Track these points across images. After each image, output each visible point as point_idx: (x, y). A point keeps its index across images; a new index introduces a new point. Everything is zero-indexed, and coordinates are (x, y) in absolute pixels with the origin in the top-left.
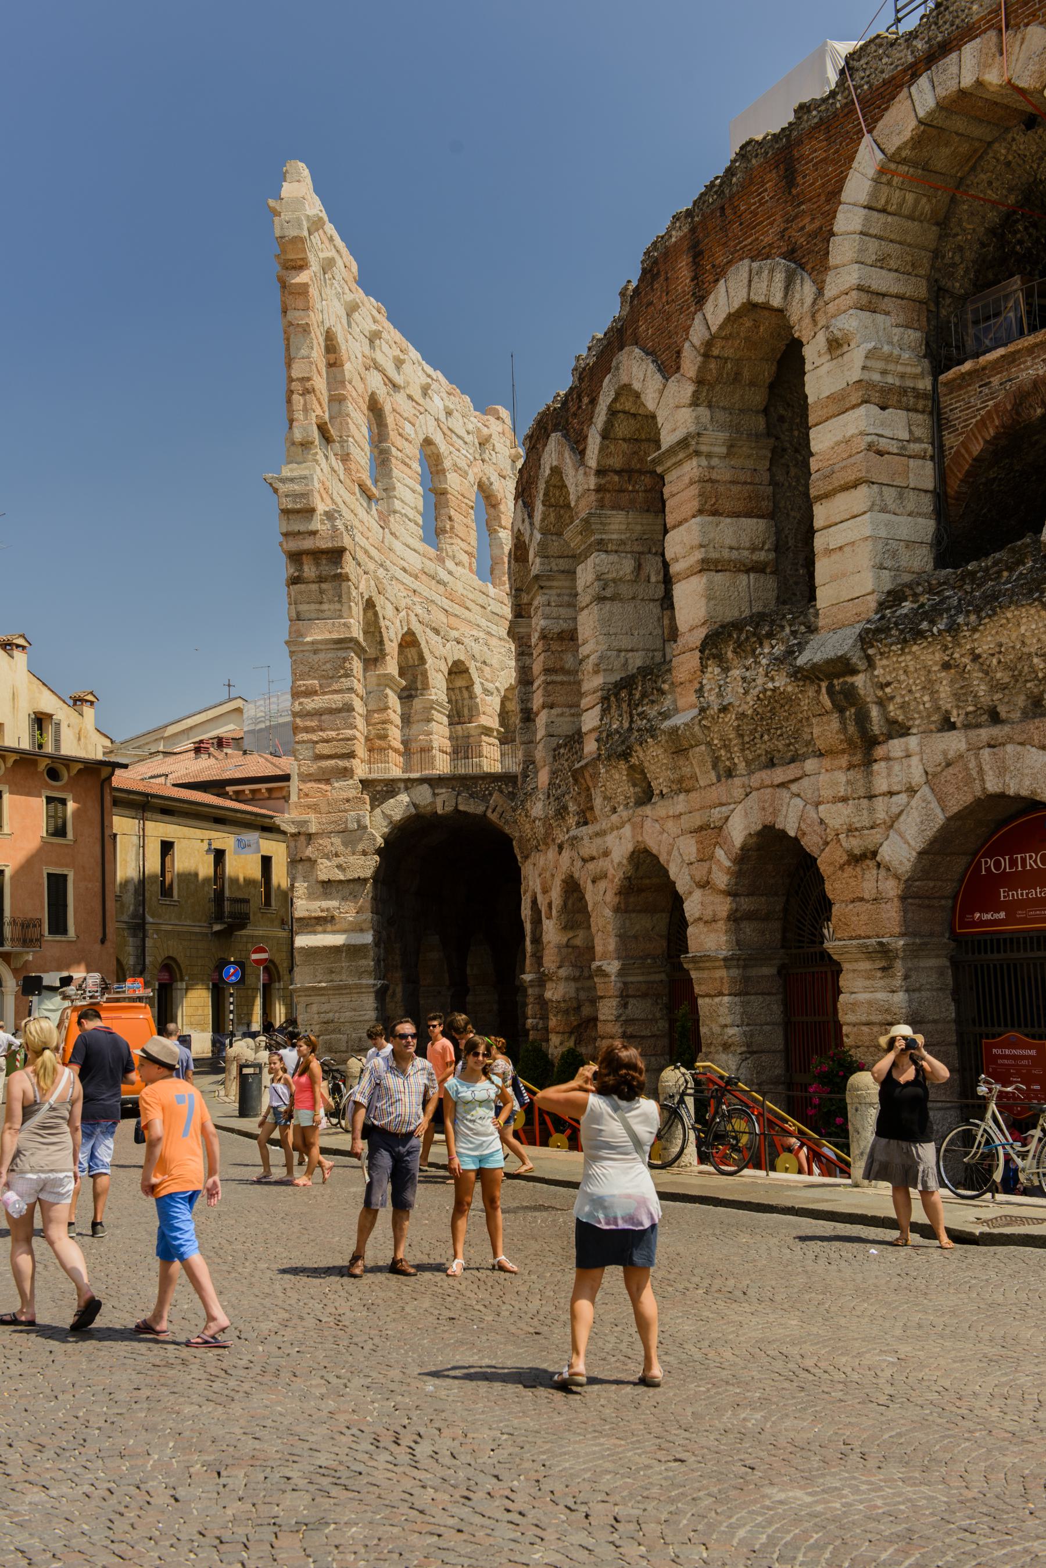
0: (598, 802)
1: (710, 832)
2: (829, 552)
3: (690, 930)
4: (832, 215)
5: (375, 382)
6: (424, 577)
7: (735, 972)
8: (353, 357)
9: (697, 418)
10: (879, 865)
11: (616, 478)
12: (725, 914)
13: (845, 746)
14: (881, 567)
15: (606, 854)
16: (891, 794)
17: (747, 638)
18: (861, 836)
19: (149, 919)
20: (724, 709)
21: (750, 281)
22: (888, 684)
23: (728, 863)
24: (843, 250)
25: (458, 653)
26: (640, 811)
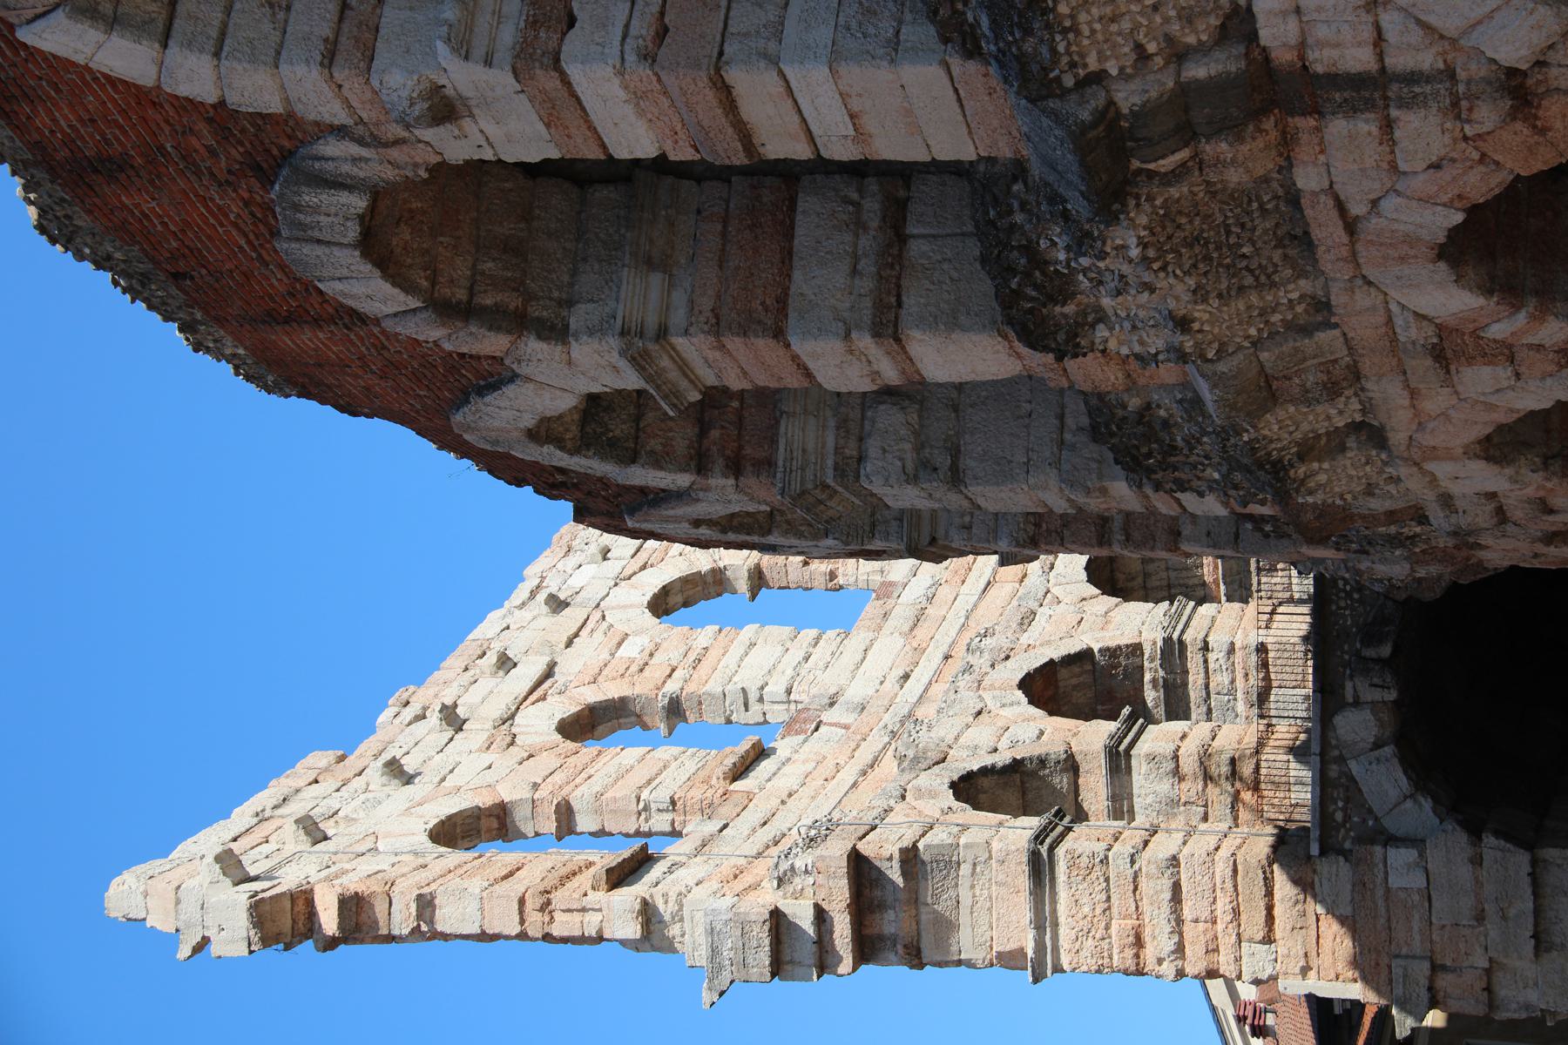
0: (1377, 505)
1: (1448, 349)
2: (860, 135)
4: (189, 105)
5: (539, 722)
6: (922, 633)
8: (490, 776)
9: (591, 332)
11: (715, 434)
13: (1269, 124)
14: (895, 43)
15: (1492, 496)
16: (1379, 39)
17: (1036, 287)
20: (1183, 324)
21: (319, 241)
22: (1139, 48)
23: (1521, 318)
24: (255, 90)
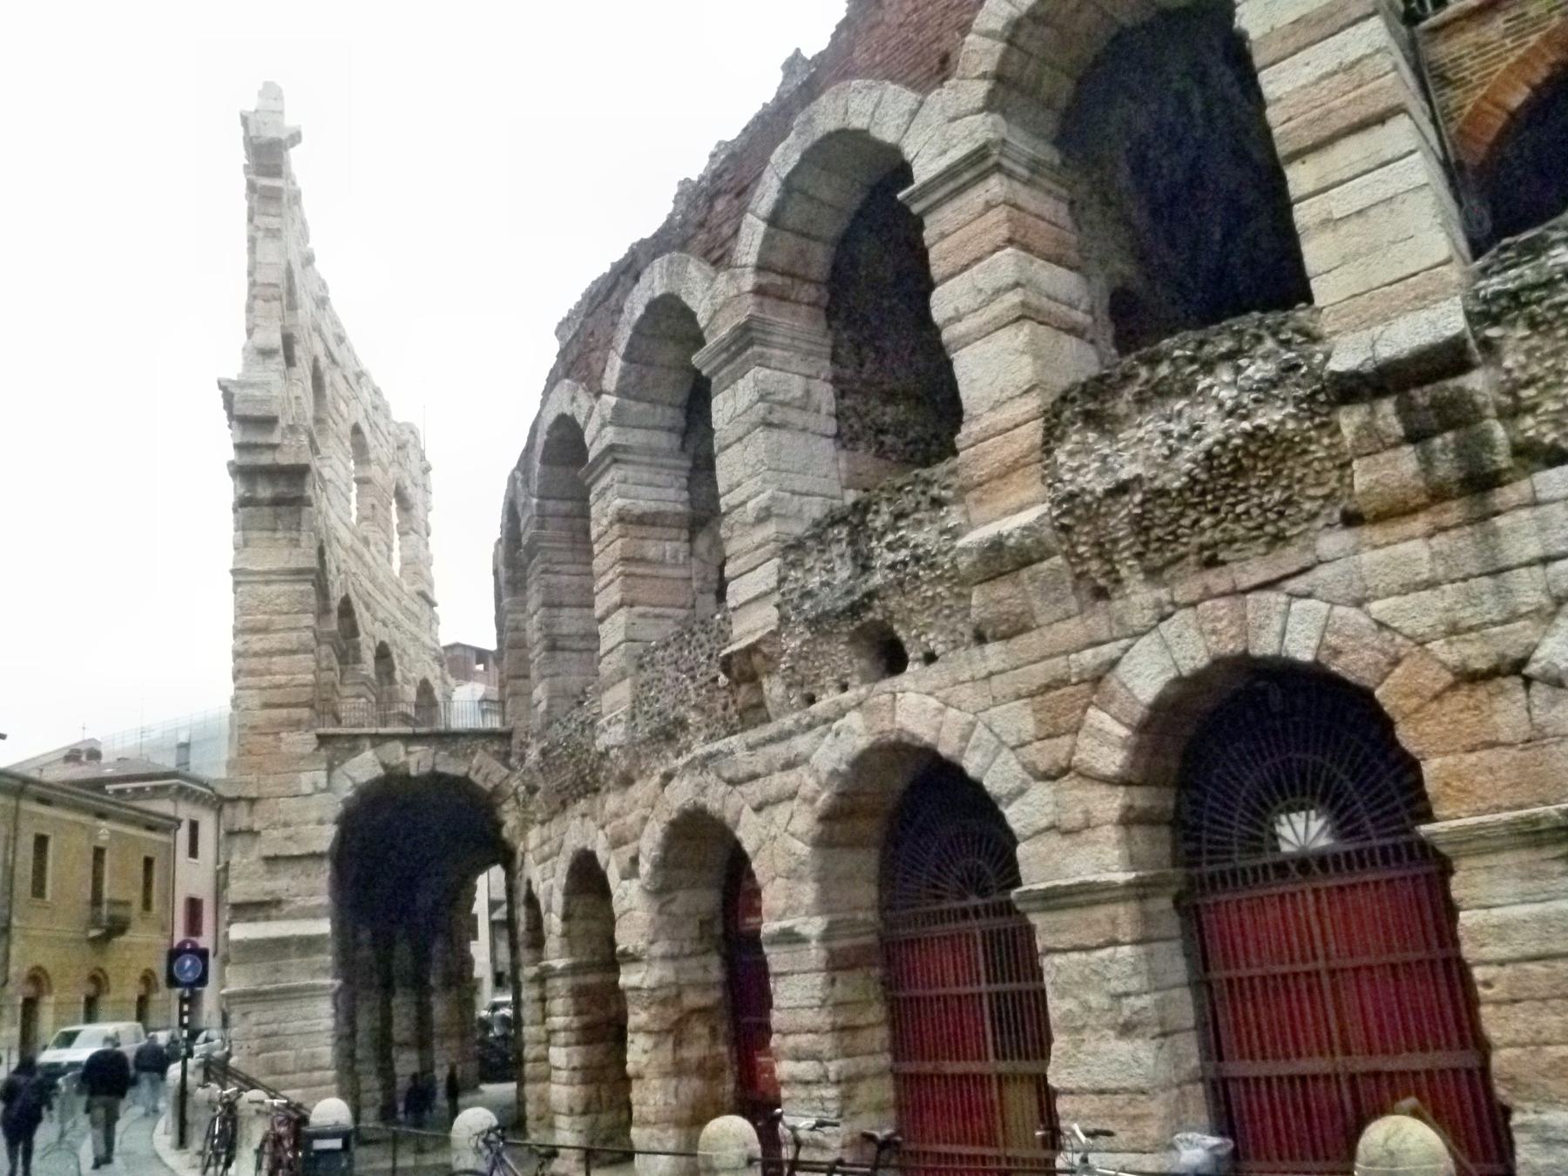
2: (1329, 223)
3: (1022, 851)
7: (1133, 906)
10: (1528, 681)
12: (1115, 815)
18: (1486, 640)
19: (15, 921)
22: (1529, 383)
23: (1124, 732)
25: (383, 635)
26: (887, 684)
